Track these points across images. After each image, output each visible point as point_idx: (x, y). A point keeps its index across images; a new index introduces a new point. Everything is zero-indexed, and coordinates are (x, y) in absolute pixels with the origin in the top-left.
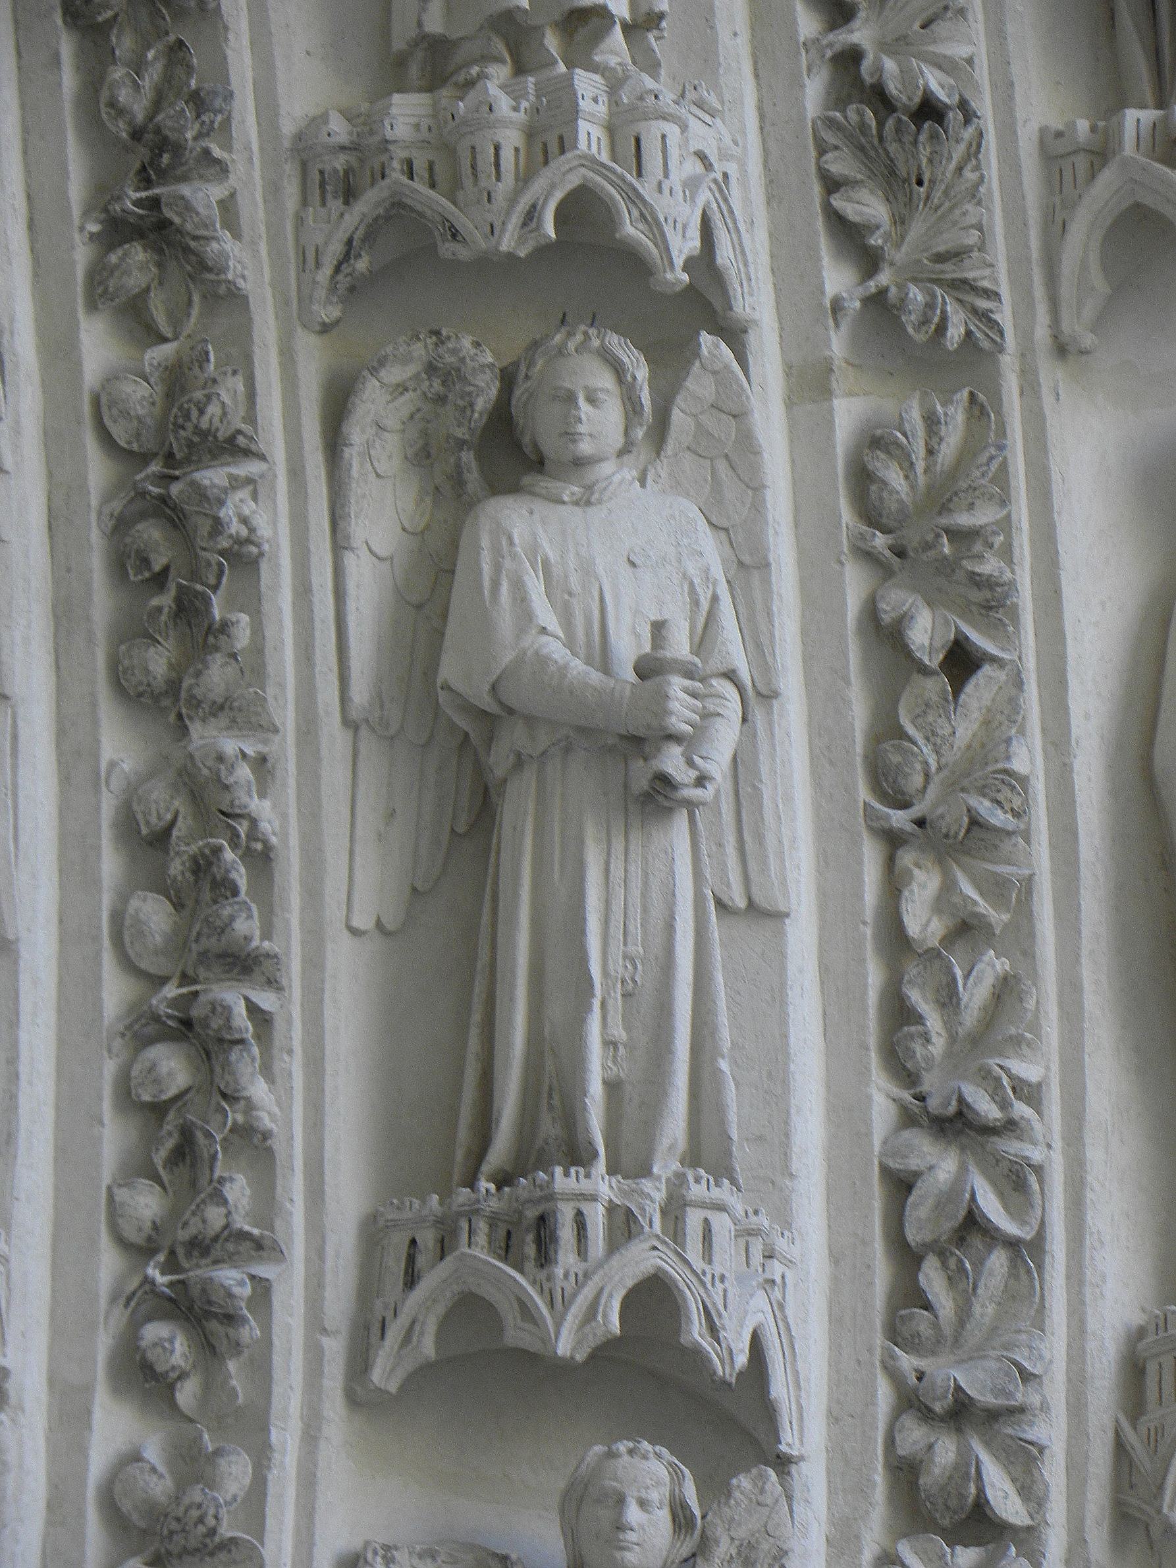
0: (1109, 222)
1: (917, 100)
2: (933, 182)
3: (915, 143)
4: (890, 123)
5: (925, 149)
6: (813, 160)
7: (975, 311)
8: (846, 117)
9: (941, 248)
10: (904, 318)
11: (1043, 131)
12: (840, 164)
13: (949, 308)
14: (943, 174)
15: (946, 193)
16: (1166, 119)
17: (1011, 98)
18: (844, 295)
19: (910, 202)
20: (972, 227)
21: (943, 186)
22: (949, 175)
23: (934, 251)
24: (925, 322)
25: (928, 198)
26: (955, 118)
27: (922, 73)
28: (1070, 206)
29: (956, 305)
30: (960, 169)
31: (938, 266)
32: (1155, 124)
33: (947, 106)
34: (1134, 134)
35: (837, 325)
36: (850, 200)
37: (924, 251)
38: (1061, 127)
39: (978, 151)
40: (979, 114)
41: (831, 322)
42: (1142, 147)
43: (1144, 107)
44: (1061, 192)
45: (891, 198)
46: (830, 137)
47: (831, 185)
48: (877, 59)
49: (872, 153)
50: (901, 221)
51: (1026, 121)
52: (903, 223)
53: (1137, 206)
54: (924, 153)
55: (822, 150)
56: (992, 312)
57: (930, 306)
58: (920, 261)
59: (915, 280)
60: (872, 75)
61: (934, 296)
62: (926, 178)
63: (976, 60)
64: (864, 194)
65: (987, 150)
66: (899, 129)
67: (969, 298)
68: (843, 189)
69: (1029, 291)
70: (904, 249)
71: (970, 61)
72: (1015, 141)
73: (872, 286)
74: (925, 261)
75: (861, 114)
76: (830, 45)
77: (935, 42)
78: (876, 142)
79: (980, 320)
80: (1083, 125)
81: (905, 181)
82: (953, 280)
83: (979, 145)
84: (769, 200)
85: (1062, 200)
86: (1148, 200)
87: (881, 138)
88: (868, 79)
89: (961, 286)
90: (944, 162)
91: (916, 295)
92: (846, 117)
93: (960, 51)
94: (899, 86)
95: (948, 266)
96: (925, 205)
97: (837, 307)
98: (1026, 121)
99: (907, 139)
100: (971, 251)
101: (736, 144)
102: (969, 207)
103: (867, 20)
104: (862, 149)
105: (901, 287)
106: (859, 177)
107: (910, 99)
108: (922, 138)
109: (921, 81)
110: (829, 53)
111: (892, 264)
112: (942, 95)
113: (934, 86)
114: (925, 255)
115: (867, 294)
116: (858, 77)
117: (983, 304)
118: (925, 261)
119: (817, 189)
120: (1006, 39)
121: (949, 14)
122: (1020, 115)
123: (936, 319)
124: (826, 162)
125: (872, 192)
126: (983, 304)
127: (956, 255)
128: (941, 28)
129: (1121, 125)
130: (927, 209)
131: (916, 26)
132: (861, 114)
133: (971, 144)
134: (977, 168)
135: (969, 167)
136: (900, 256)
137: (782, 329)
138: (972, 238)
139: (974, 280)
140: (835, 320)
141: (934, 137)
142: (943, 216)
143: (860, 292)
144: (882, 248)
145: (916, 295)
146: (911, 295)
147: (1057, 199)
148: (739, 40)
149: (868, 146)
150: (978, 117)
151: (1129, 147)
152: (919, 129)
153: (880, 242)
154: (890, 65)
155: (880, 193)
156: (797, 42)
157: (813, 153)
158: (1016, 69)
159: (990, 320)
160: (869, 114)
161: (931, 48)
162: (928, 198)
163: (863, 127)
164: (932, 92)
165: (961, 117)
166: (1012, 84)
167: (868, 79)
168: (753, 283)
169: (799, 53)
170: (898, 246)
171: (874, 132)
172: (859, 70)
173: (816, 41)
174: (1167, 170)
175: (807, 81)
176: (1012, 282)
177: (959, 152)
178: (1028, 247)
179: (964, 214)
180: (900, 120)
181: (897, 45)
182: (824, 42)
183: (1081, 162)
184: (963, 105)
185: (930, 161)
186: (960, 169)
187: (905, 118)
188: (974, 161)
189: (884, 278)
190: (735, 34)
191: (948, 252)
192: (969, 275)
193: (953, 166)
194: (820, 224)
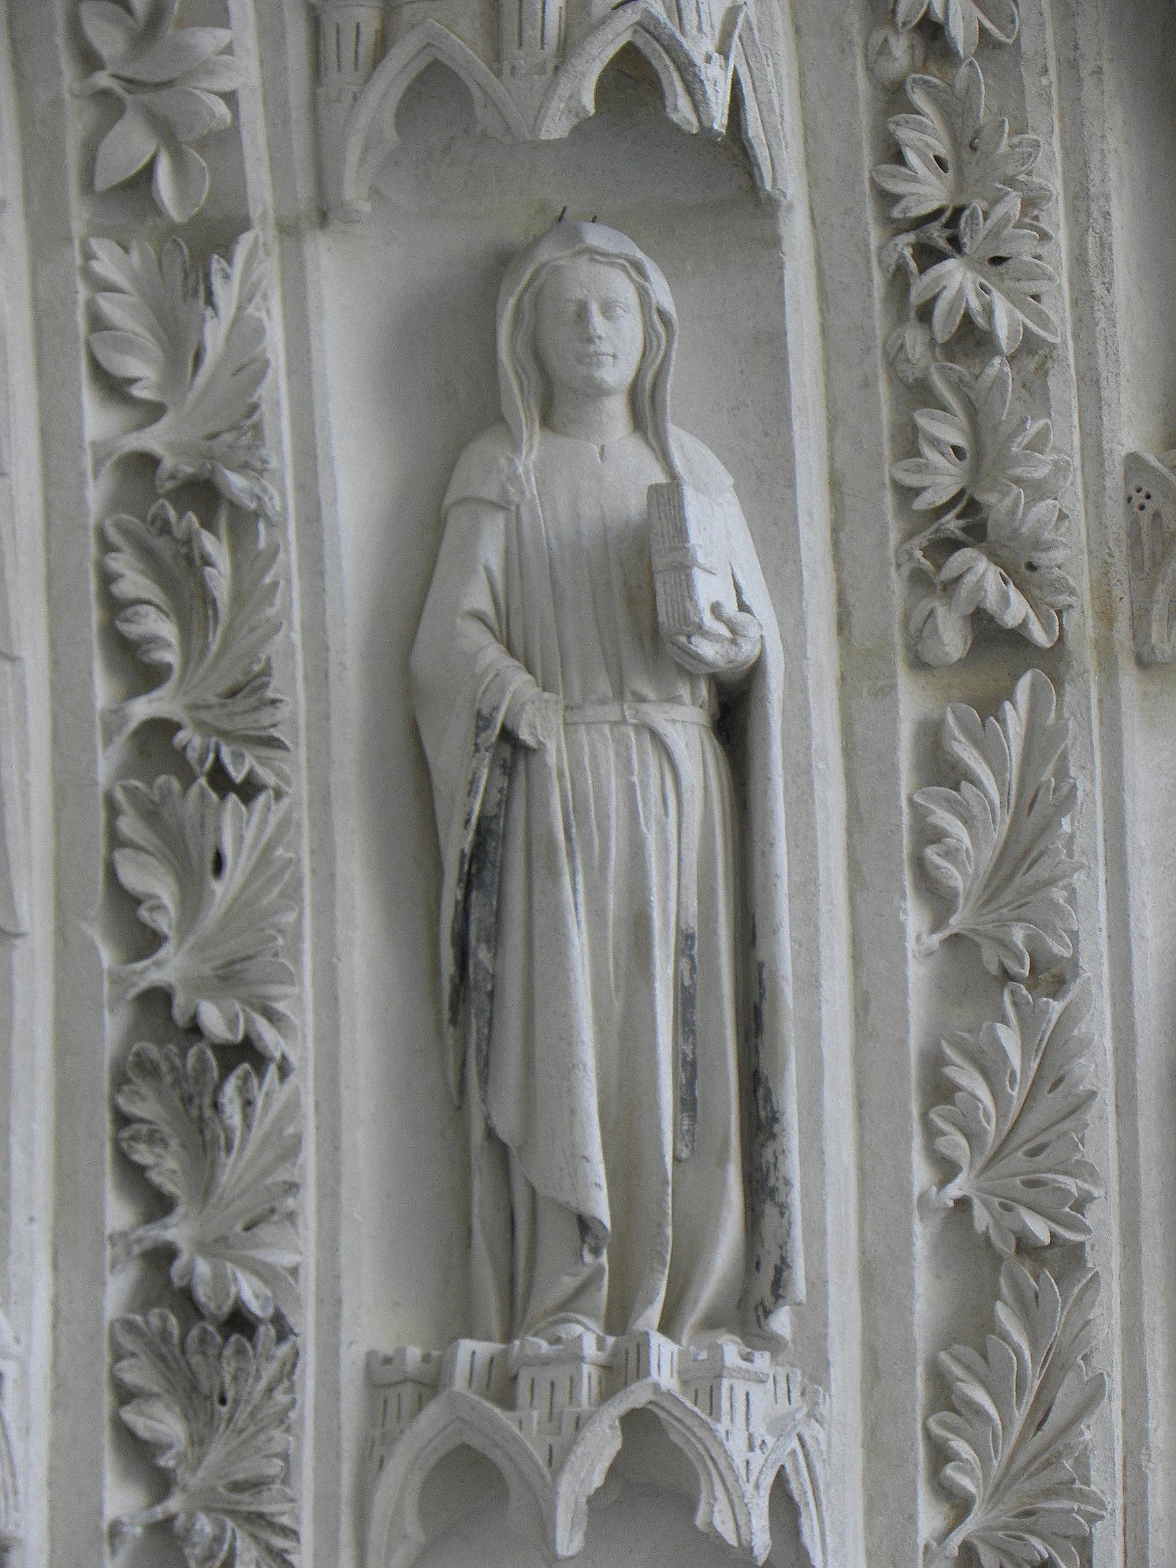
0: (432, 1462)
1: (227, 1309)
2: (237, 1402)
3: (219, 1356)
4: (195, 1332)
5: (229, 1365)
6: (106, 1368)
7: (269, 1549)
8: (147, 1322)
9: (240, 1477)
10: (187, 1551)
11: (371, 1355)
12: (135, 1374)
13: (239, 1544)
14: (250, 1394)
15: (252, 1415)
16: (505, 1354)
17: (338, 1316)
18: (125, 1519)
19: (211, 1422)
20: (277, 1455)
21: (249, 1408)
22: (257, 1396)
23: (230, 1479)
24: (210, 1556)
25: (230, 1420)
26: (266, 1335)
27: (235, 1279)
28: (389, 1440)
29: (249, 1541)
30: (270, 1390)
31: (235, 1497)
32: (492, 1359)
33: (259, 1320)
34: (468, 1367)
35: (114, 1552)
36: (142, 1414)
37: (220, 1478)
38: (390, 1353)
39: (292, 1372)
40: (296, 1331)
41: (106, 1548)
42: (475, 1383)
43: (489, 1338)
44: (383, 1425)
45: (191, 1415)
46: (128, 1343)
47: (125, 1395)
48: (192, 1260)
49: (174, 1365)
50: (199, 1441)
51: (351, 1343)
52: (202, 1444)
53: (465, 1448)
54: (228, 1369)
55: (118, 1354)
56: (286, 1551)
57: (218, 1539)
58: (214, 1489)
59: (208, 1510)
60: (182, 1277)
61: (223, 1528)
62: (230, 1395)
63: (301, 1270)
64: (158, 1409)
65: (304, 1372)
66: (204, 1336)
67: (265, 1534)
68: (135, 1401)
69: (335, 1532)
70: (201, 1473)
71: (294, 1271)
72: (337, 1364)
73: (159, 1512)
74: (221, 1490)
75: (164, 1319)
76: (139, 1240)
77: (257, 1247)
78: (177, 1352)
79: (274, 1561)
80: (414, 1353)
81: (208, 1398)
82: (249, 1513)
83: (294, 1366)
84: (56, 1405)
85: (383, 1436)
86: (476, 1442)
87: (183, 1350)
88: (177, 1282)
89: (257, 1520)
90: (250, 1382)
91: (205, 1525)
92: (147, 1322)
93: (283, 1259)
94: (210, 1294)
95: (245, 1497)
96: (227, 1427)
97: (115, 1531)
98: (351, 1343)
99: (212, 1352)
100: (273, 1482)
101: (17, 1340)
102: (277, 1433)
103: (186, 1216)
104: (163, 1358)
105: (191, 1516)
106: (155, 1389)
107: (219, 1308)
108: (228, 1351)
109: (233, 1290)
110: (137, 1250)
111: (184, 1489)
112: (255, 1307)
113: (248, 1296)
114: (222, 1482)
115: (152, 1521)
116: (169, 1281)
117: (279, 1542)
118: (221, 1490)
119: (107, 1398)
120: (338, 1250)
121: (276, 1218)
122: (345, 1336)
123: (222, 1555)
124: (120, 1370)
125: (168, 1407)
126: (279, 1542)
127: (256, 1485)
128: (265, 1232)
129: (454, 1356)
130: (228, 1432)
131: (239, 1228)
132: (164, 1319)
133: (284, 1364)
134: (291, 1390)
135: (281, 1389)
136: (194, 1481)
137: (53, 1551)
138: (274, 1467)
139: (273, 1515)
140: (112, 1545)
141: (240, 1352)
142: (246, 1441)
143: (145, 1517)
144: (173, 1471)
145: (205, 1525)
146: (198, 1526)
147: (378, 1432)
148: (35, 1227)
149: (169, 1356)
150: (296, 1335)
151: (459, 1382)
152: (226, 1338)
153: (171, 1463)
154: (203, 1268)
155: (177, 1409)
156: (102, 1234)
157: (107, 1358)
158: (347, 1284)
159: (285, 1561)
160: (173, 1320)
161: (252, 1253)
162: (230, 1420)
163: (165, 1334)
164: (244, 1303)
165: (273, 1332)
166: (339, 1301)
167: (177, 1282)
168: (21, 1498)
169: (103, 1247)
170: (194, 1469)
171: (176, 1340)
172: (169, 1270)
173: (124, 1235)
174: (497, 1411)
175: (109, 1279)
176: (318, 1519)
177: (269, 1371)
178: (339, 1484)
179: (270, 1440)
180: (205, 1330)
181: (204, 1247)
182: (133, 1236)
183: (408, 1393)
184: (278, 1319)
185: (235, 1378)
186: (270, 1390)
187: (211, 1328)
188: (286, 1383)
189: (174, 1504)
190: (32, 1220)
191: (246, 1481)
192: (267, 1509)
193: (262, 1385)
194: (106, 1437)
